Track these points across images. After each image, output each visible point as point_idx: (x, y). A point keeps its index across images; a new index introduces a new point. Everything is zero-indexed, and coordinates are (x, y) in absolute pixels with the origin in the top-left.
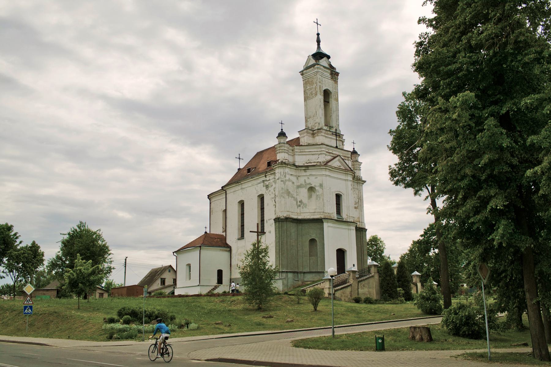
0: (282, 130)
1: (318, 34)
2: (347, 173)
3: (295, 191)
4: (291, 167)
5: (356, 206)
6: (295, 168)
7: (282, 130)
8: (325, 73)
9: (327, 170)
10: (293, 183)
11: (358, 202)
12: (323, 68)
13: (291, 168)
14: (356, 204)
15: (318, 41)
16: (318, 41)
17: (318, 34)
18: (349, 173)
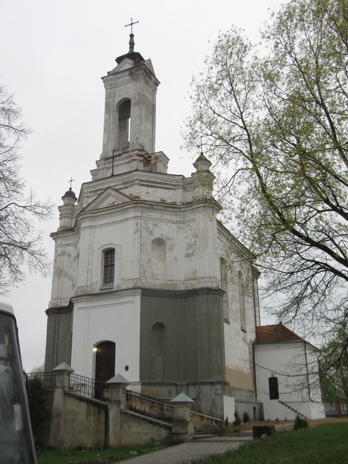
0: (71, 189)
1: (132, 36)
2: (124, 208)
3: (72, 265)
4: (65, 235)
5: (190, 251)
6: (72, 233)
7: (71, 189)
8: (117, 81)
9: (85, 220)
10: (70, 255)
11: (195, 242)
12: (114, 77)
13: (66, 236)
14: (189, 246)
15: (132, 44)
16: (132, 44)
17: (132, 36)
18: (126, 207)
